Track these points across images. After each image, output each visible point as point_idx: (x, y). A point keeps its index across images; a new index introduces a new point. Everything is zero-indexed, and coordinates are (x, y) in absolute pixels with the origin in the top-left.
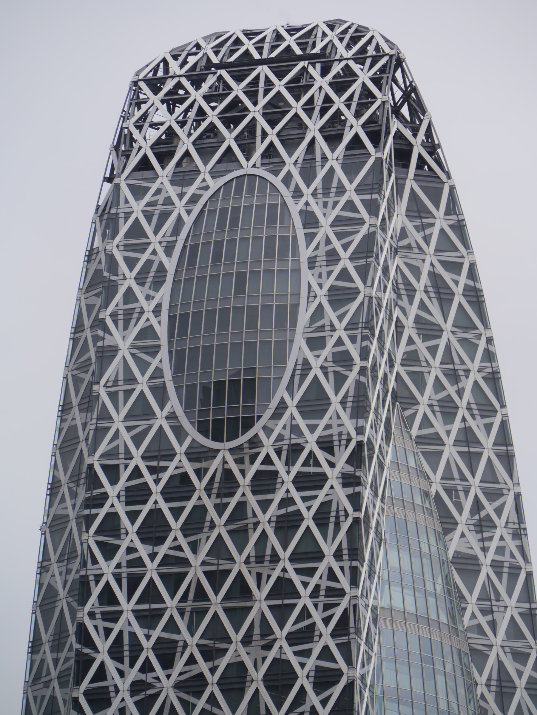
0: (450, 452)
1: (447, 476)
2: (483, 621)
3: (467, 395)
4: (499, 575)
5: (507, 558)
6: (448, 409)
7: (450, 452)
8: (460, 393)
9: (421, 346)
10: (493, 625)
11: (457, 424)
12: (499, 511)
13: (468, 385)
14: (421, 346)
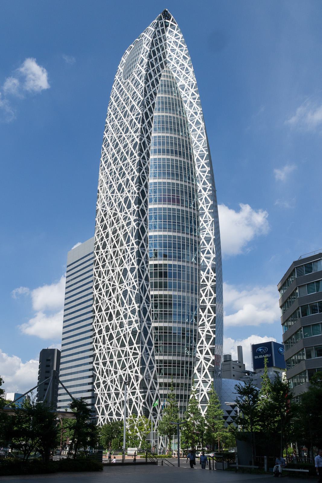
1: (178, 72)
2: (186, 95)
3: (182, 58)
4: (189, 86)
5: (191, 83)
9: (172, 54)
10: (188, 95)
11: (180, 64)
13: (182, 57)
14: (172, 54)
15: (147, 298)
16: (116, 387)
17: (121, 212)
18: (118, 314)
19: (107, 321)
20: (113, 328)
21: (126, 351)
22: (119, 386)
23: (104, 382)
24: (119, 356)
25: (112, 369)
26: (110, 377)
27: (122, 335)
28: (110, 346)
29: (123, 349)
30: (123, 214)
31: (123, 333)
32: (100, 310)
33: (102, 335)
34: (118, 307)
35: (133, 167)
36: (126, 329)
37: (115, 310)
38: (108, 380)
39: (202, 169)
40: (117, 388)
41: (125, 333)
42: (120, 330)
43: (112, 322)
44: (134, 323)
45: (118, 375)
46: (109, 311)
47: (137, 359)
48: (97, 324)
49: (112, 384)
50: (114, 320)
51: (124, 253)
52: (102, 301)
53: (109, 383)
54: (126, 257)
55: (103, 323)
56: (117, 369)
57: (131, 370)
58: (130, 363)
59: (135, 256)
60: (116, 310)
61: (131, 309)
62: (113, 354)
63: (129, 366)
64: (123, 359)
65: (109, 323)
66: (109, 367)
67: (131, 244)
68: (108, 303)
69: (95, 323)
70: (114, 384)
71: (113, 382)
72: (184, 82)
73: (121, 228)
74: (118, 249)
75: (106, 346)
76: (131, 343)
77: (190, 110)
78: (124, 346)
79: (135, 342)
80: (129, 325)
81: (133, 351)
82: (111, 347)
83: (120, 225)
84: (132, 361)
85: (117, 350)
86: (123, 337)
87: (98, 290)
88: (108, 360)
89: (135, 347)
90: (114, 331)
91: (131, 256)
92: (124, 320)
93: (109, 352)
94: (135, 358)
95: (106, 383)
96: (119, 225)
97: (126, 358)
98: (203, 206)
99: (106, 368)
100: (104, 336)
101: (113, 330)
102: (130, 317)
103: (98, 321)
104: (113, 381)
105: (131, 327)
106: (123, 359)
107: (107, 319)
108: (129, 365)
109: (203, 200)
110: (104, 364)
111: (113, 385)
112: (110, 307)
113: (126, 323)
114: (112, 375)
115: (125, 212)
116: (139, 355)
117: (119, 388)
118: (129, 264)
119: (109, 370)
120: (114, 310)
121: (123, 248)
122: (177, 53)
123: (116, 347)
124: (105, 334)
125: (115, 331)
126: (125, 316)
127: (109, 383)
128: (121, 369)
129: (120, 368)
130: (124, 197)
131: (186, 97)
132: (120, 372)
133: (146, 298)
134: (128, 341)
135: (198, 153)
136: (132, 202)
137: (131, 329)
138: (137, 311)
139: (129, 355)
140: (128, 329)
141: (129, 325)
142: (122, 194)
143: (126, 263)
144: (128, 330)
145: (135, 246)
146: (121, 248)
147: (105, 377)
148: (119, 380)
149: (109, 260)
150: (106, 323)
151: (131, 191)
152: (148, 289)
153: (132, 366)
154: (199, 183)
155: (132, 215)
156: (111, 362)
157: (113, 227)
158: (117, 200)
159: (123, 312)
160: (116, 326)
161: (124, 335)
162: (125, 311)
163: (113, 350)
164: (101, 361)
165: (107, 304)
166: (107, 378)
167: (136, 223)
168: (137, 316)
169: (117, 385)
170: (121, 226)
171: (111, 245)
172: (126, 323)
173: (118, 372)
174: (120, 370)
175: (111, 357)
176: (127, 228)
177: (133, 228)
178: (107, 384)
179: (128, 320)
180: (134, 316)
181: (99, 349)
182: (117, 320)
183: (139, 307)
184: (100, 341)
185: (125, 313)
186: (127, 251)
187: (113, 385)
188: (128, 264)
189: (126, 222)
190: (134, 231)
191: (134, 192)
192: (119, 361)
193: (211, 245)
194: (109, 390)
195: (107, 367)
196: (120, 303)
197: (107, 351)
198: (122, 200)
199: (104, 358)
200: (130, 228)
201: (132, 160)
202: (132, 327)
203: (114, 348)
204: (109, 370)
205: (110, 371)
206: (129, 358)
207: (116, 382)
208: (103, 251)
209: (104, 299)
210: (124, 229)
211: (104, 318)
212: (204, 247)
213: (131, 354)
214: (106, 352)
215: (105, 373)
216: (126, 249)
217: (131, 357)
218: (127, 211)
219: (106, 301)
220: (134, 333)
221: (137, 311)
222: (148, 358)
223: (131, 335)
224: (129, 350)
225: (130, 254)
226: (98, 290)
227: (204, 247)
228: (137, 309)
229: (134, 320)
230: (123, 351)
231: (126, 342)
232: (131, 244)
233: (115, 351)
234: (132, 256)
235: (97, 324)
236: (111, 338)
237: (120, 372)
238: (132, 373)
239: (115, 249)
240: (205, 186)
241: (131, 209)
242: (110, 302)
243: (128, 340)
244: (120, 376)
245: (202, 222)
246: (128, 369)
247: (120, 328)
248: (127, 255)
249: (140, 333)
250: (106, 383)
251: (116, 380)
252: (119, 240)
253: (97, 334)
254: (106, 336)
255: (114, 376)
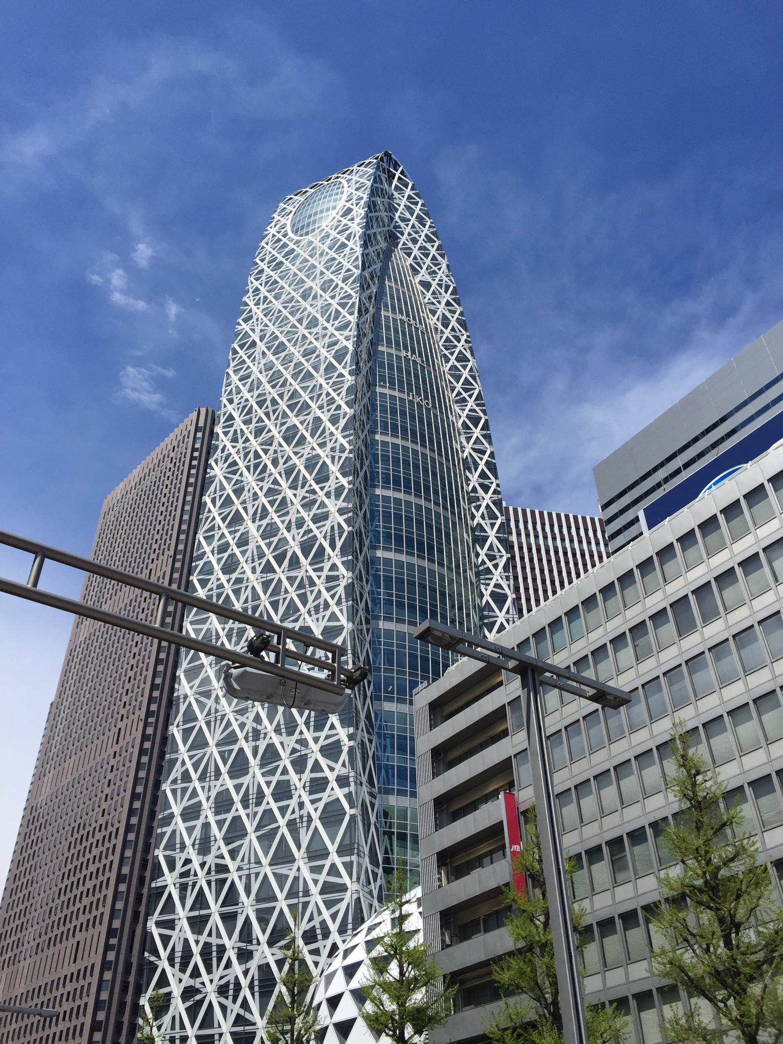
0: (416, 252)
3: (423, 237)
6: (415, 241)
7: (416, 252)
8: (420, 236)
10: (439, 302)
12: (439, 269)
13: (423, 235)
15: (368, 717)
16: (242, 1012)
17: (296, 489)
18: (271, 755)
19: (225, 776)
20: (245, 803)
21: (296, 879)
22: (254, 1006)
23: (188, 993)
24: (266, 895)
25: (231, 944)
26: (218, 973)
27: (282, 822)
28: (228, 861)
29: (282, 870)
30: (301, 492)
31: (288, 816)
32: (200, 743)
33: (199, 823)
34: (273, 735)
35: (334, 395)
36: (301, 805)
37: (258, 743)
38: (207, 983)
39: (476, 447)
40: (248, 1016)
41: (296, 815)
42: (274, 806)
43: (246, 780)
44: (333, 784)
45: (253, 965)
46: (236, 748)
47: (342, 906)
48: (180, 785)
49: (223, 1000)
50: (256, 774)
51: (301, 586)
52: (209, 714)
53: (213, 997)
54: (311, 598)
55: (206, 785)
56: (250, 942)
57: (313, 946)
58: (311, 919)
59: (343, 596)
60: (262, 745)
61: (321, 742)
62: (240, 887)
63: (305, 932)
64: (282, 904)
65: (230, 784)
66: (219, 936)
67: (327, 566)
68: (233, 721)
69: (175, 781)
70: (234, 1001)
71: (231, 992)
72: (428, 278)
73: (294, 526)
74: (281, 573)
75: (211, 860)
76: (317, 853)
77: (444, 330)
78: (289, 859)
79: (332, 848)
80: (311, 793)
81: (323, 877)
82: (232, 865)
83: (292, 516)
84: (320, 913)
85: (257, 874)
86: (284, 830)
87: (197, 682)
88: (215, 908)
89: (333, 866)
90: (249, 811)
91: (326, 595)
92: (293, 776)
93: (224, 880)
94: (329, 904)
95: (198, 997)
96: (287, 518)
97: (295, 901)
98: (482, 522)
99: (203, 938)
100: (206, 826)
101: (246, 806)
102: (317, 767)
103: (186, 777)
104: (231, 986)
105: (320, 799)
106: (282, 904)
107: (224, 769)
108: (304, 926)
109: (483, 509)
110: (198, 924)
111: (228, 1003)
112: (240, 735)
113: (299, 785)
114: (228, 965)
115: (307, 488)
116: (349, 893)
117: (256, 1017)
118: (320, 615)
119: (218, 946)
120: (254, 744)
121: (300, 574)
122: (413, 226)
123: (253, 865)
124: (212, 819)
125: (256, 809)
126: (299, 764)
127: (213, 997)
128: (271, 943)
129: (263, 939)
130: (305, 456)
131: (433, 303)
132: (265, 954)
133: (366, 717)
134: (304, 845)
135: (466, 412)
136: (334, 469)
137: (321, 805)
138: (345, 750)
139: (307, 893)
140: (307, 804)
141: (311, 793)
142: (296, 450)
143: (309, 612)
144: (309, 807)
145: (342, 570)
146: (293, 574)
147: (196, 974)
148: (256, 983)
149: (246, 601)
150: (219, 783)
151: (330, 445)
152: (369, 694)
153: (319, 931)
154: (471, 472)
155: (333, 497)
156: (229, 919)
157: (265, 522)
158: (281, 461)
159: (289, 750)
160: (260, 795)
161: (291, 825)
162: (298, 747)
163: (241, 873)
164: (182, 913)
165: (229, 724)
166: (205, 977)
167: (345, 516)
168: (344, 765)
169: (245, 1005)
170: (293, 520)
171: (256, 564)
172: (299, 785)
173: (257, 956)
174: (265, 946)
175: (231, 898)
176: (313, 526)
177: (336, 528)
178: (201, 1002)
179: (307, 775)
180: (332, 764)
181: (179, 869)
182: (263, 775)
183: (351, 737)
184: (188, 842)
185: (298, 754)
186: (312, 583)
187: (228, 1003)
188: (314, 617)
189: (312, 513)
190: (340, 537)
191: (338, 448)
192: (263, 917)
193: (508, 612)
194: (208, 1021)
195: (210, 935)
196: (282, 722)
197: (213, 879)
198: (300, 464)
199: (201, 901)
200: (327, 528)
201: (331, 381)
202: (325, 797)
203: (245, 867)
204: (214, 948)
205: (222, 949)
206: (306, 904)
207: (246, 992)
208: (224, 579)
209: (217, 711)
210: (305, 528)
211: (212, 768)
212: (491, 614)
213: (314, 890)
214: (209, 883)
215: (197, 959)
216: (310, 578)
217: (316, 898)
218: (316, 487)
219: (223, 716)
220: (332, 814)
221: (345, 750)
222: (371, 906)
223: (317, 823)
224: (306, 873)
225: (324, 591)
226: (197, 682)
227: (491, 614)
228: (346, 743)
229: (331, 776)
230: (281, 879)
231: (299, 848)
232: (327, 566)
233: (248, 877)
234: (333, 597)
235: (180, 785)
236: (236, 832)
237: (265, 954)
238: (316, 958)
239: (270, 576)
240: (486, 482)
241: (331, 485)
242: (242, 719)
243: (305, 840)
244: (264, 969)
245: (482, 557)
246: (300, 942)
247: (276, 800)
248: (312, 592)
249: (353, 817)
250: (198, 997)
251: (245, 983)
252: (284, 554)
253: (178, 819)
254: (214, 828)
255: (237, 968)
